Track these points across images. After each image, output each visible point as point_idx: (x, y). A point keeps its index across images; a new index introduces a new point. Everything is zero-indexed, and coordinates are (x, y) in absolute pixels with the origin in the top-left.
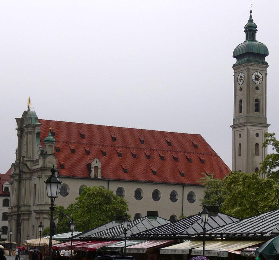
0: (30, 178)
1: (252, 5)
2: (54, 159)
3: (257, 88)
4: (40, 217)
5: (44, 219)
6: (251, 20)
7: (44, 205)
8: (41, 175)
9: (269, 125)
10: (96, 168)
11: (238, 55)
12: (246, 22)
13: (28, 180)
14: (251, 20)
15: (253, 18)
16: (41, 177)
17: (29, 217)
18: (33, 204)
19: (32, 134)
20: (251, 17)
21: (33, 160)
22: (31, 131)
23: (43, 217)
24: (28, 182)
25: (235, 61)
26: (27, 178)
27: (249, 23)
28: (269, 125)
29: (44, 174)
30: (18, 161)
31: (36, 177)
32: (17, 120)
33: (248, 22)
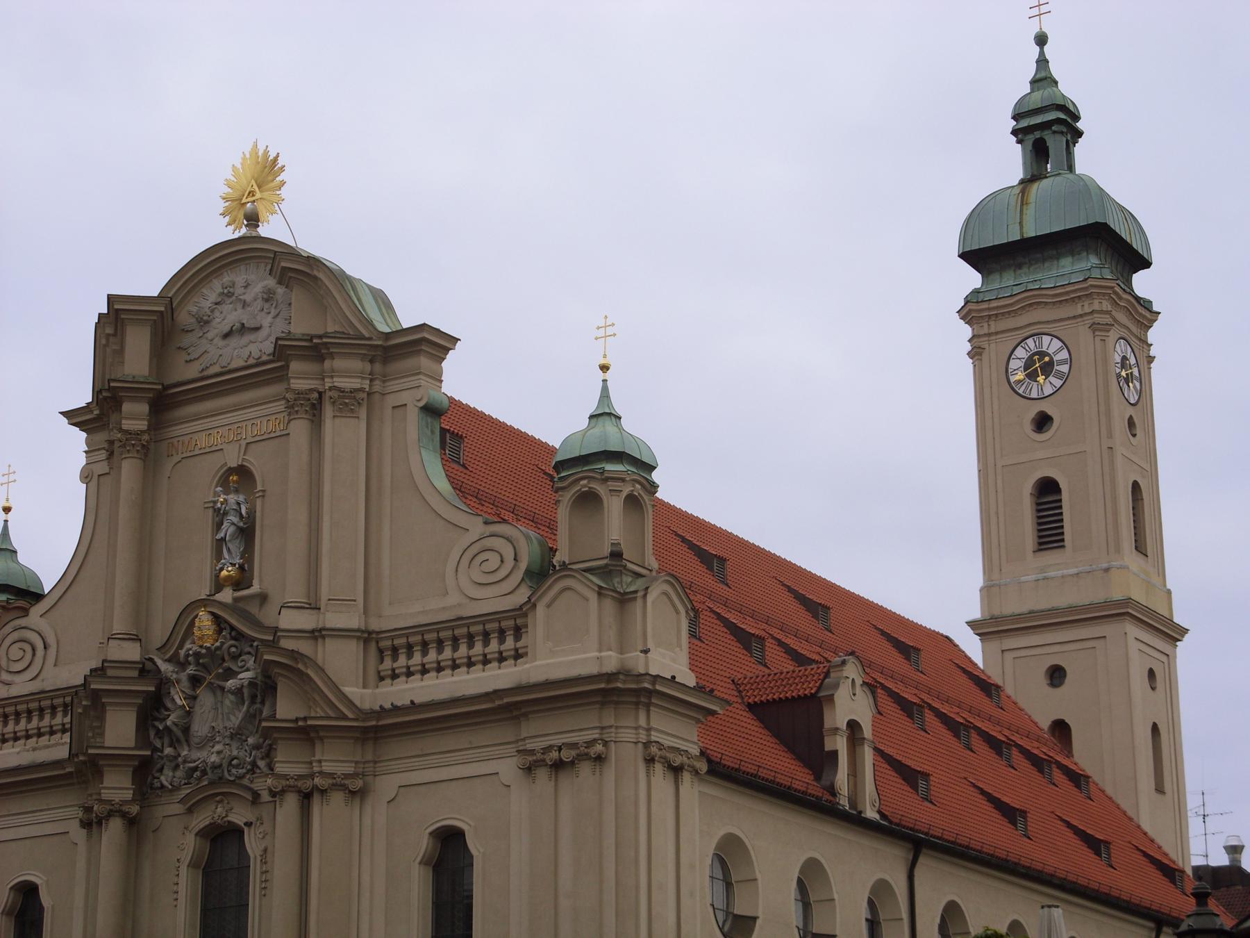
0: (357, 784)
2: (677, 612)
3: (1131, 423)
6: (1043, 78)
8: (606, 743)
9: (1185, 631)
10: (853, 726)
14: (1043, 78)
15: (1055, 70)
16: (599, 759)
19: (363, 413)
20: (1042, 62)
21: (375, 625)
22: (354, 383)
25: (972, 279)
27: (1032, 90)
28: (1185, 631)
29: (628, 735)
31: (508, 768)
33: (1027, 89)
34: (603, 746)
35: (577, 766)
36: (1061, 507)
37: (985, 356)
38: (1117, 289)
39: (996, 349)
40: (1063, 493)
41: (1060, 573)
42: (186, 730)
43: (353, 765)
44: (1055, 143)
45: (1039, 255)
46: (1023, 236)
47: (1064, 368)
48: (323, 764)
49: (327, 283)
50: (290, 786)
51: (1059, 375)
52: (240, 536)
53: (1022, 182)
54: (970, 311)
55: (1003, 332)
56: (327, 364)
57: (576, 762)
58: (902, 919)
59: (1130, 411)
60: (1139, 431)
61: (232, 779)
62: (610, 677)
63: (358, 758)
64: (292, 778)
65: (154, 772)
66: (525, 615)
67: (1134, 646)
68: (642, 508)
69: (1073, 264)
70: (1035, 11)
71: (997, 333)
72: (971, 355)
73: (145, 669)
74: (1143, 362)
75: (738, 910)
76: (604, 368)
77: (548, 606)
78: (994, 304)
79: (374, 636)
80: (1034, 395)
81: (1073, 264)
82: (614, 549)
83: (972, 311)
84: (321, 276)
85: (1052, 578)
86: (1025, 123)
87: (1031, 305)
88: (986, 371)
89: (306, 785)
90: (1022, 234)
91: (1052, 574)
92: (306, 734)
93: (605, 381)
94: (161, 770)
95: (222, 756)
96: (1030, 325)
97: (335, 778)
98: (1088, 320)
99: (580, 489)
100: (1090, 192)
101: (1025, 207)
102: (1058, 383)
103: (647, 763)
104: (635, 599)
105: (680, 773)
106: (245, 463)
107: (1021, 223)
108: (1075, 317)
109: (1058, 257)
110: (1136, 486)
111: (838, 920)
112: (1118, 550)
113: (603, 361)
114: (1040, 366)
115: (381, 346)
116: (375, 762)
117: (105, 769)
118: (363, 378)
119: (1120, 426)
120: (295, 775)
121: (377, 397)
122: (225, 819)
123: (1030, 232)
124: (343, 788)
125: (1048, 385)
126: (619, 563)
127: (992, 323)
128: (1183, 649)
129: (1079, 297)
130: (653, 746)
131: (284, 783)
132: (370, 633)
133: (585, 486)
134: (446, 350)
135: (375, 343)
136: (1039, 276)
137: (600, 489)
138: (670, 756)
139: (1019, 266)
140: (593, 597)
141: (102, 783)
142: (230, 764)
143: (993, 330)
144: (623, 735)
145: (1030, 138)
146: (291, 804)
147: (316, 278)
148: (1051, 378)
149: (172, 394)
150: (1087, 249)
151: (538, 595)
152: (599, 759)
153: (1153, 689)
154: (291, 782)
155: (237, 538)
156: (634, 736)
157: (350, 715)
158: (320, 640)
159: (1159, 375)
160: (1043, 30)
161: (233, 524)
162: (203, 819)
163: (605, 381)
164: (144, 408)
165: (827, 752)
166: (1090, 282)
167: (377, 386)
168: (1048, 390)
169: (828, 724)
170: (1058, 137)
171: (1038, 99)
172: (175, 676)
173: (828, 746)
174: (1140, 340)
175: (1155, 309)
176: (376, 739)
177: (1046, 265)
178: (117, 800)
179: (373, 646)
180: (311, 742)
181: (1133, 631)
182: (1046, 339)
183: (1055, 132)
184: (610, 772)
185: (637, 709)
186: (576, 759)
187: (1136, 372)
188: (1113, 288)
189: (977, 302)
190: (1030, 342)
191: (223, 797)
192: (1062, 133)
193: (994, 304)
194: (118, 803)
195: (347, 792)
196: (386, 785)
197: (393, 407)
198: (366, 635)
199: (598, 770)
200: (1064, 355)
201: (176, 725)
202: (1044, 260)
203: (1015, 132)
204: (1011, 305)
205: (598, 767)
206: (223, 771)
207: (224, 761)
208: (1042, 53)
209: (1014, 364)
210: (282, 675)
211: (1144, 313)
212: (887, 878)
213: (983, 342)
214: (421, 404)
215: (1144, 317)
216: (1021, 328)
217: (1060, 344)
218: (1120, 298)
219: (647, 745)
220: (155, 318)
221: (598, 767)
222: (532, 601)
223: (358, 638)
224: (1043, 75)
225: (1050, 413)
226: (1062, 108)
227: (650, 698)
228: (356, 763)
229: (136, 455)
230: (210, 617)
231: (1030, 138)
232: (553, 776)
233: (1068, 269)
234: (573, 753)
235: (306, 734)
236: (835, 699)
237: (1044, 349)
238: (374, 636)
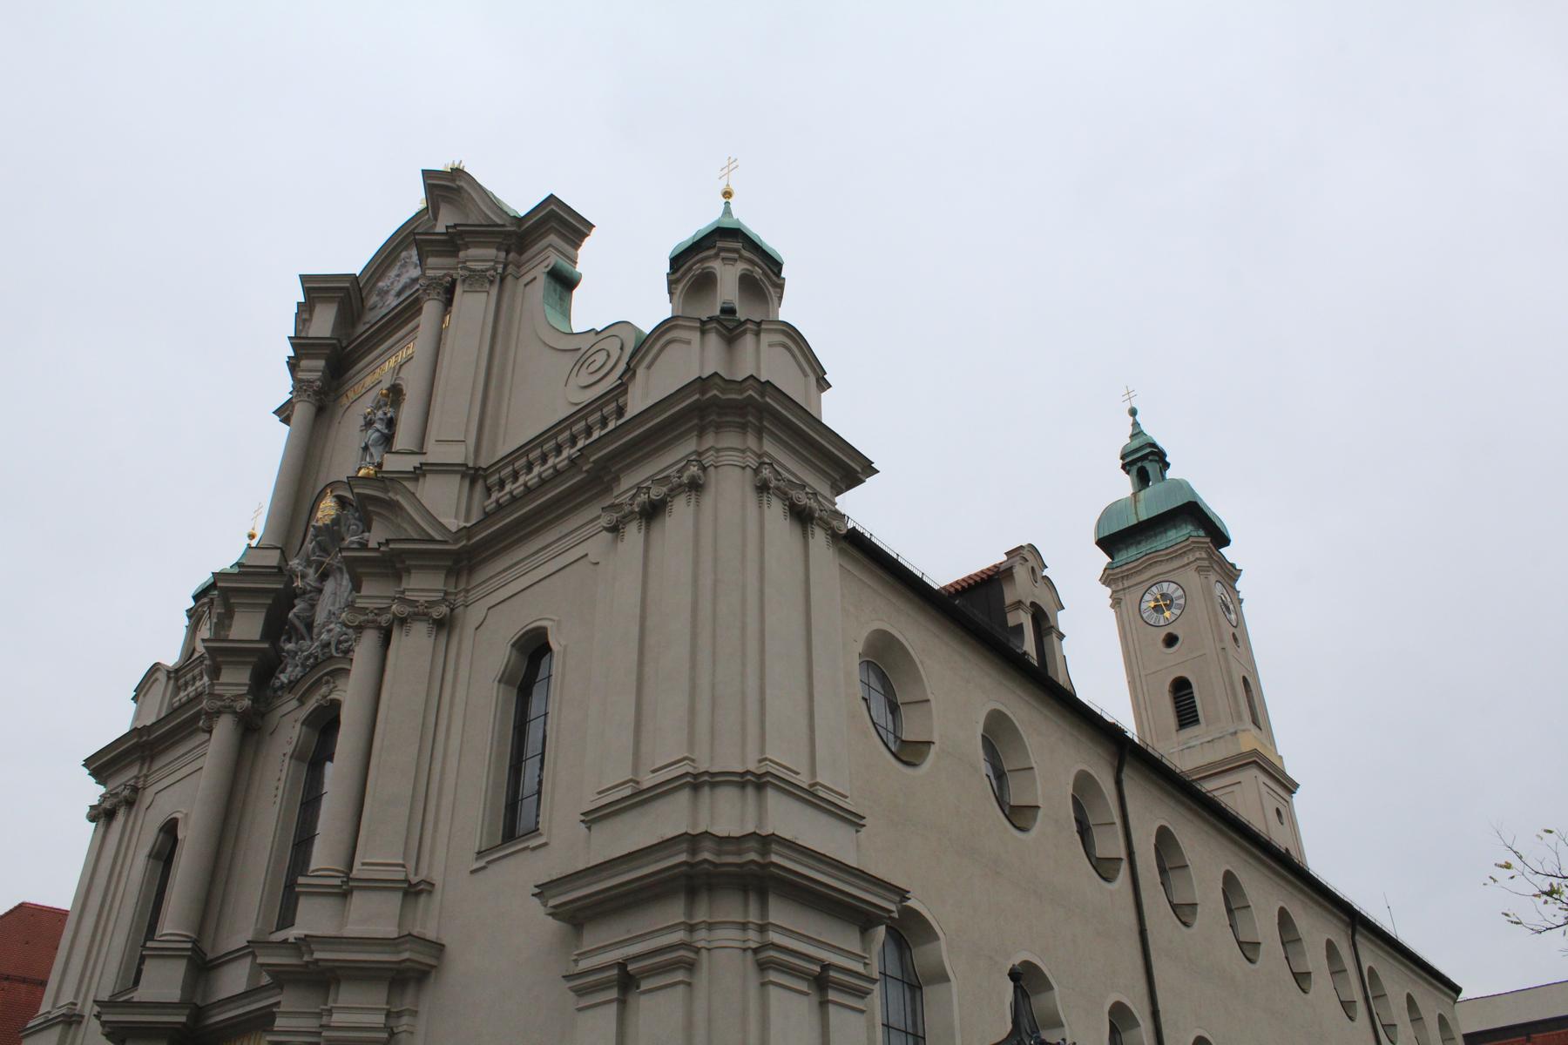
0: (444, 609)
1: (1131, 395)
3: (1235, 639)
4: (701, 938)
5: (763, 966)
6: (1137, 432)
7: (757, 783)
8: (704, 469)
11: (1136, 522)
12: (1123, 439)
13: (420, 630)
14: (1137, 432)
16: (695, 486)
17: (388, 1014)
18: (480, 854)
20: (1136, 424)
23: (753, 939)
24: (412, 645)
26: (412, 603)
27: (1131, 441)
28: (1297, 786)
29: (734, 458)
30: (272, 559)
32: (317, 289)
34: (698, 469)
35: (670, 504)
36: (1193, 697)
37: (1123, 603)
38: (1211, 545)
39: (1130, 599)
40: (1193, 686)
41: (1198, 742)
42: (310, 626)
43: (442, 595)
44: (1151, 468)
45: (1152, 533)
46: (1138, 519)
47: (1182, 601)
48: (407, 593)
49: (469, 191)
50: (368, 621)
52: (385, 444)
53: (1133, 494)
54: (1109, 575)
56: (462, 254)
57: (669, 499)
58: (1114, 823)
59: (1234, 630)
60: (1240, 643)
61: (340, 655)
62: (702, 383)
63: (452, 590)
64: (372, 612)
65: (278, 671)
66: (625, 392)
67: (1264, 789)
68: (767, 297)
70: (1127, 397)
71: (1129, 587)
72: (1112, 606)
73: (280, 571)
74: (1236, 603)
75: (907, 736)
76: (727, 194)
77: (649, 367)
78: (1125, 568)
79: (481, 472)
82: (725, 305)
83: (1108, 578)
84: (462, 184)
85: (1194, 746)
87: (1150, 564)
88: (1125, 615)
89: (384, 620)
90: (1138, 519)
92: (393, 564)
93: (727, 203)
94: (283, 671)
95: (331, 634)
96: (1152, 577)
97: (417, 607)
98: (1194, 566)
99: (693, 276)
100: (1181, 485)
101: (1138, 504)
102: (1178, 612)
103: (758, 493)
104: (744, 332)
105: (809, 525)
106: (397, 382)
107: (1136, 513)
108: (1184, 566)
109: (1165, 531)
110: (1245, 679)
111: (1039, 792)
112: (1240, 718)
113: (722, 186)
115: (514, 232)
116: (467, 591)
117: (223, 667)
118: (497, 262)
119: (1228, 638)
120: (376, 609)
121: (509, 278)
122: (329, 698)
123: (1144, 517)
124: (425, 618)
126: (731, 318)
127: (1125, 582)
128: (1297, 798)
129: (1185, 552)
130: (766, 469)
131: (362, 618)
132: (477, 469)
133: (697, 269)
134: (583, 236)
135: (509, 229)
136: (1155, 544)
137: (716, 266)
138: (794, 493)
139: (1139, 543)
140: (695, 337)
141: (218, 680)
142: (339, 642)
143: (1126, 585)
144: (724, 458)
145: (1134, 469)
146: (369, 640)
147: (459, 190)
148: (1173, 610)
149: (350, 350)
150: (1186, 522)
151: (638, 358)
152: (695, 486)
153: (1282, 824)
154: (371, 617)
155: (381, 445)
156: (741, 460)
157: (438, 537)
159: (1246, 608)
160: (1134, 406)
161: (378, 430)
162: (312, 704)
163: (727, 203)
164: (321, 363)
165: (1011, 627)
166: (1191, 539)
167: (510, 269)
169: (1009, 598)
170: (1154, 463)
171: (1137, 443)
172: (300, 568)
173: (1012, 620)
174: (1232, 587)
175: (1238, 568)
176: (471, 570)
177: (1158, 538)
178: (228, 695)
179: (479, 487)
180: (398, 577)
181: (1263, 778)
182: (1165, 585)
183: (1151, 461)
184: (708, 499)
185: (744, 433)
186: (669, 495)
187: (1231, 607)
188: (1207, 543)
189: (1113, 569)
190: (1154, 589)
191: (329, 678)
192: (1156, 461)
193: (1125, 568)
194: (228, 698)
195: (431, 621)
196: (475, 614)
197: (526, 285)
198: (472, 472)
199: (693, 500)
200: (1180, 592)
201: (298, 617)
202: (1156, 535)
203: (1124, 467)
204: (1138, 566)
205: (693, 497)
206: (331, 650)
207: (333, 639)
208: (1135, 420)
209: (1144, 606)
210: (379, 514)
211: (1230, 574)
212: (1092, 772)
213: (1120, 595)
214: (548, 269)
215: (1232, 572)
216: (1147, 580)
217: (1175, 586)
218: (1214, 553)
219: (756, 471)
220: (342, 295)
221: (693, 497)
222: (632, 366)
223: (463, 477)
224: (1137, 431)
225: (1175, 632)
226: (1153, 445)
227: (760, 420)
228: (446, 593)
229: (306, 399)
230: (334, 500)
231: (1134, 469)
232: (643, 527)
234: (665, 489)
235: (393, 564)
236: (1015, 575)
237: (1165, 591)
238: (481, 472)
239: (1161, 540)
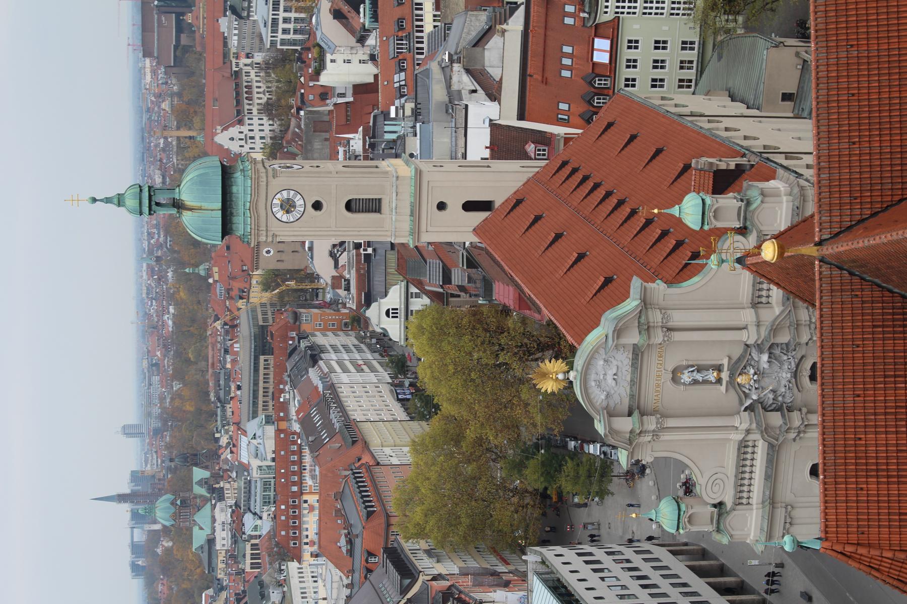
11: (220, 212)
20: (108, 200)
41: (394, 201)
51: (295, 196)
55: (267, 223)
69: (237, 186)
71: (267, 226)
80: (302, 209)
81: (237, 186)
86: (146, 209)
91: (394, 205)
96: (266, 209)
98: (270, 178)
102: (299, 196)
107: (212, 210)
108: (267, 186)
114: (288, 206)
123: (219, 205)
125: (299, 201)
127: (261, 229)
139: (232, 214)
143: (264, 229)
158: (761, 323)
168: (302, 202)
182: (275, 201)
190: (274, 210)
193: (253, 227)
202: (232, 201)
208: (101, 200)
209: (284, 219)
216: (267, 214)
230: (740, 376)
231: (154, 207)
233: (241, 189)
239: (237, 198)
